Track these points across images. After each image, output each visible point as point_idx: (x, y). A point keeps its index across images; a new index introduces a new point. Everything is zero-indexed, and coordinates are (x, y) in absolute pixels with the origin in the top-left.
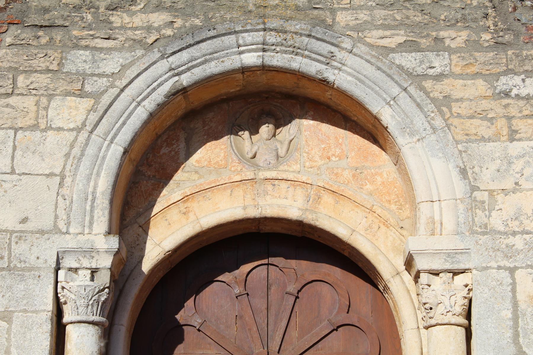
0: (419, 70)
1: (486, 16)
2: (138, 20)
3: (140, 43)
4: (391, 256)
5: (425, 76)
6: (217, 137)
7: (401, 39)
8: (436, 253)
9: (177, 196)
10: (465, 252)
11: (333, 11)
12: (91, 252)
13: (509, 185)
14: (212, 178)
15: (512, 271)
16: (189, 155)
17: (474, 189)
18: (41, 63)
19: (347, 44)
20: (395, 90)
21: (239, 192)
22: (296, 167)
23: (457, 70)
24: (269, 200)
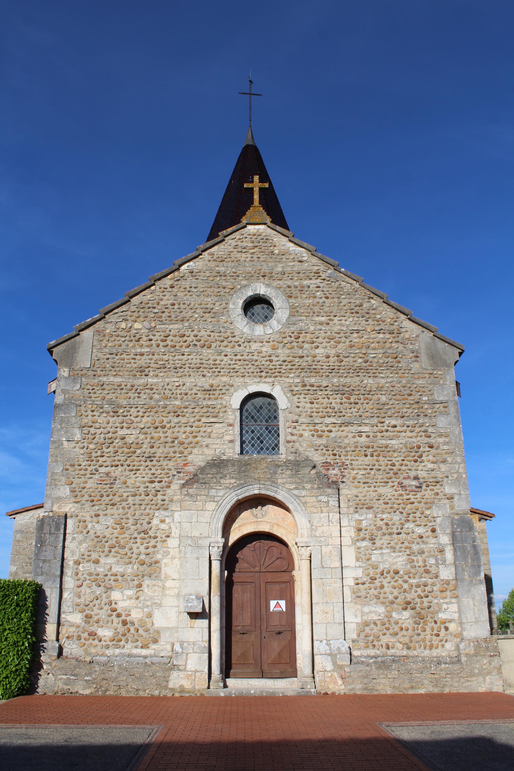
0: (299, 495)
1: (316, 480)
2: (227, 481)
3: (228, 487)
4: (292, 541)
5: (300, 496)
6: (247, 510)
7: (294, 487)
8: (303, 542)
9: (237, 526)
10: (310, 542)
11: (277, 479)
12: (217, 542)
13: (321, 525)
14: (246, 521)
15: (321, 546)
16: (240, 515)
17: (312, 526)
18: (203, 493)
19: (281, 488)
20: (293, 500)
21: (253, 524)
22: (267, 518)
23: (308, 495)
24: (261, 527)
